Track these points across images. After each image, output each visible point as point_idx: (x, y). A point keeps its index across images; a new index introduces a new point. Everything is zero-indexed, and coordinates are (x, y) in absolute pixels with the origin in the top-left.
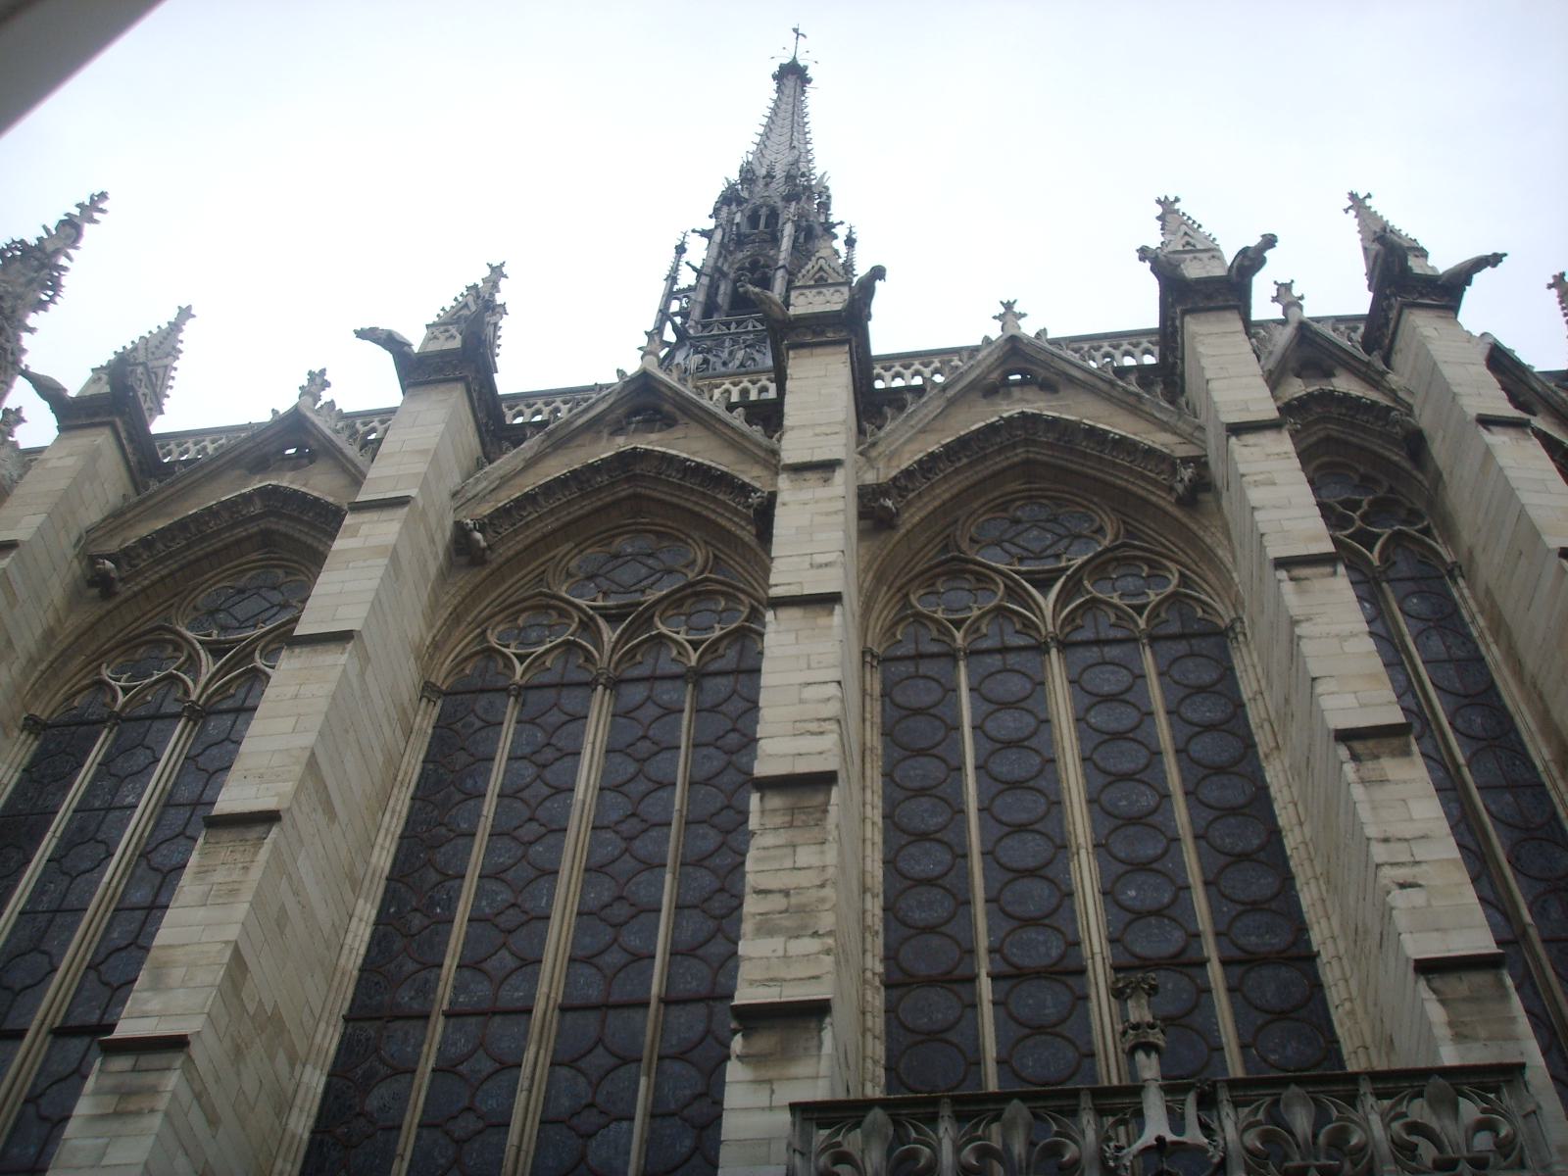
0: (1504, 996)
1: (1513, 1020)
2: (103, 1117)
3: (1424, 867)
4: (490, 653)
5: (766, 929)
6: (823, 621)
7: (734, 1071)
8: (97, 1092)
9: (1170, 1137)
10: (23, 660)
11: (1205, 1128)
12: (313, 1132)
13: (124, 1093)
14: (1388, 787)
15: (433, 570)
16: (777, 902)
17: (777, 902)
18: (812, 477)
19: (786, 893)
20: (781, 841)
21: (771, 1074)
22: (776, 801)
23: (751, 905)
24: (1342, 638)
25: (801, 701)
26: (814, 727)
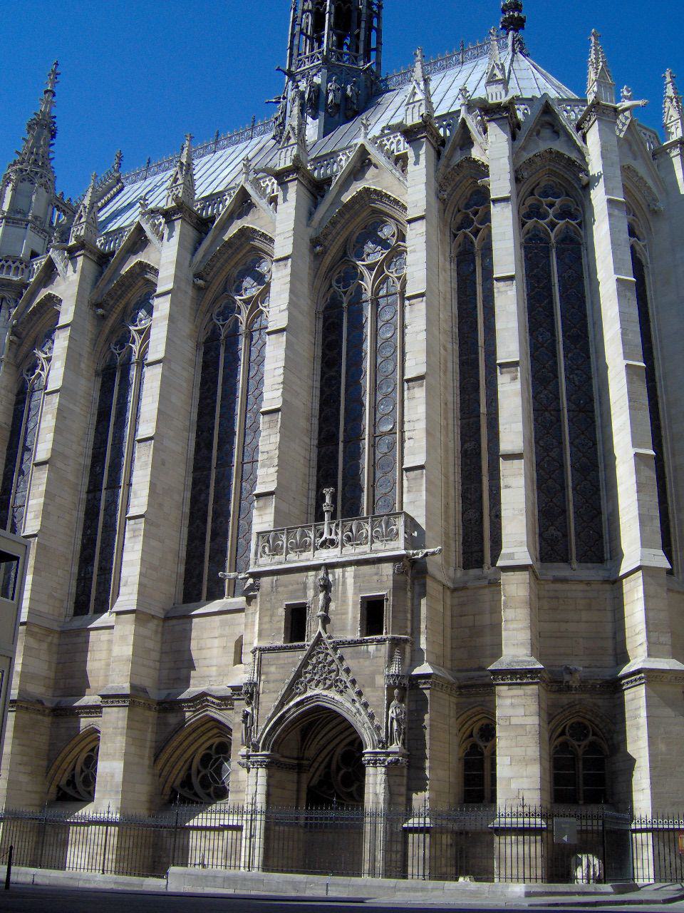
0: (422, 477)
1: (422, 485)
2: (131, 538)
3: (416, 431)
4: (215, 325)
5: (263, 466)
6: (281, 339)
7: (255, 512)
8: (129, 531)
9: (329, 537)
10: (86, 356)
11: (336, 534)
12: (190, 509)
13: (134, 531)
14: (415, 400)
15: (188, 302)
16: (265, 456)
17: (265, 456)
18: (281, 263)
19: (268, 452)
20: (267, 434)
21: (262, 513)
22: (267, 418)
23: (261, 457)
24: (417, 333)
25: (274, 376)
26: (276, 387)
